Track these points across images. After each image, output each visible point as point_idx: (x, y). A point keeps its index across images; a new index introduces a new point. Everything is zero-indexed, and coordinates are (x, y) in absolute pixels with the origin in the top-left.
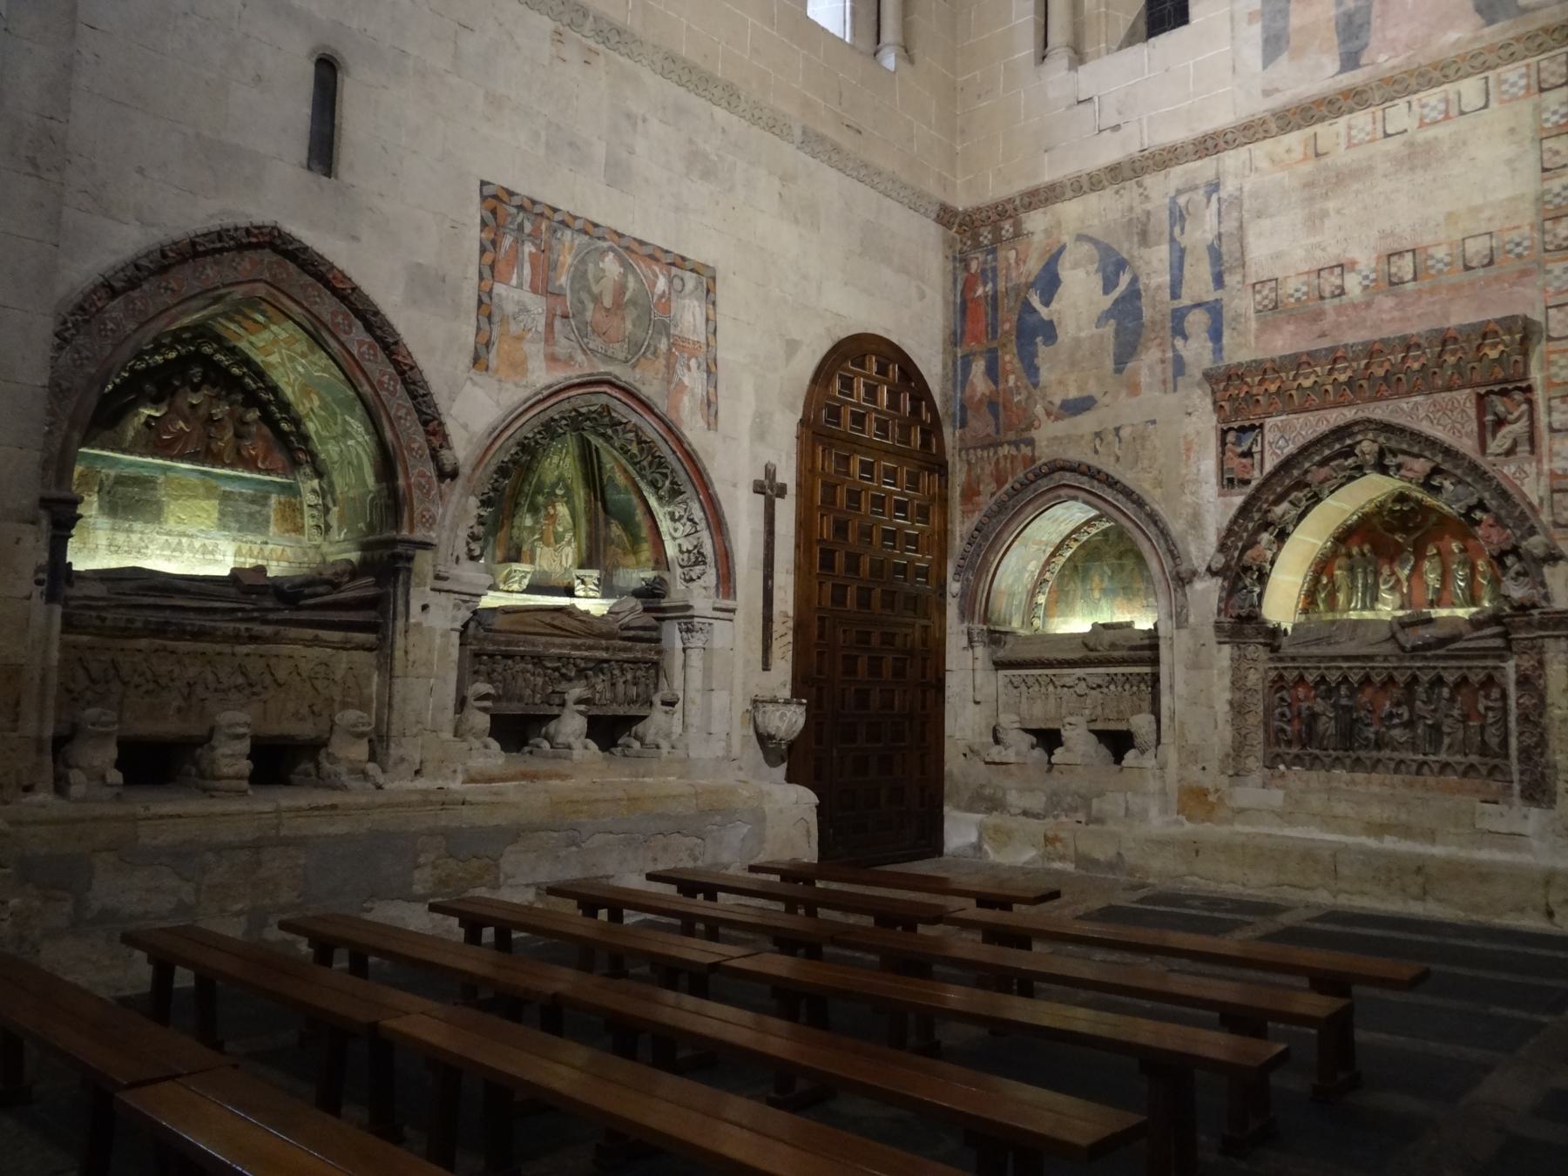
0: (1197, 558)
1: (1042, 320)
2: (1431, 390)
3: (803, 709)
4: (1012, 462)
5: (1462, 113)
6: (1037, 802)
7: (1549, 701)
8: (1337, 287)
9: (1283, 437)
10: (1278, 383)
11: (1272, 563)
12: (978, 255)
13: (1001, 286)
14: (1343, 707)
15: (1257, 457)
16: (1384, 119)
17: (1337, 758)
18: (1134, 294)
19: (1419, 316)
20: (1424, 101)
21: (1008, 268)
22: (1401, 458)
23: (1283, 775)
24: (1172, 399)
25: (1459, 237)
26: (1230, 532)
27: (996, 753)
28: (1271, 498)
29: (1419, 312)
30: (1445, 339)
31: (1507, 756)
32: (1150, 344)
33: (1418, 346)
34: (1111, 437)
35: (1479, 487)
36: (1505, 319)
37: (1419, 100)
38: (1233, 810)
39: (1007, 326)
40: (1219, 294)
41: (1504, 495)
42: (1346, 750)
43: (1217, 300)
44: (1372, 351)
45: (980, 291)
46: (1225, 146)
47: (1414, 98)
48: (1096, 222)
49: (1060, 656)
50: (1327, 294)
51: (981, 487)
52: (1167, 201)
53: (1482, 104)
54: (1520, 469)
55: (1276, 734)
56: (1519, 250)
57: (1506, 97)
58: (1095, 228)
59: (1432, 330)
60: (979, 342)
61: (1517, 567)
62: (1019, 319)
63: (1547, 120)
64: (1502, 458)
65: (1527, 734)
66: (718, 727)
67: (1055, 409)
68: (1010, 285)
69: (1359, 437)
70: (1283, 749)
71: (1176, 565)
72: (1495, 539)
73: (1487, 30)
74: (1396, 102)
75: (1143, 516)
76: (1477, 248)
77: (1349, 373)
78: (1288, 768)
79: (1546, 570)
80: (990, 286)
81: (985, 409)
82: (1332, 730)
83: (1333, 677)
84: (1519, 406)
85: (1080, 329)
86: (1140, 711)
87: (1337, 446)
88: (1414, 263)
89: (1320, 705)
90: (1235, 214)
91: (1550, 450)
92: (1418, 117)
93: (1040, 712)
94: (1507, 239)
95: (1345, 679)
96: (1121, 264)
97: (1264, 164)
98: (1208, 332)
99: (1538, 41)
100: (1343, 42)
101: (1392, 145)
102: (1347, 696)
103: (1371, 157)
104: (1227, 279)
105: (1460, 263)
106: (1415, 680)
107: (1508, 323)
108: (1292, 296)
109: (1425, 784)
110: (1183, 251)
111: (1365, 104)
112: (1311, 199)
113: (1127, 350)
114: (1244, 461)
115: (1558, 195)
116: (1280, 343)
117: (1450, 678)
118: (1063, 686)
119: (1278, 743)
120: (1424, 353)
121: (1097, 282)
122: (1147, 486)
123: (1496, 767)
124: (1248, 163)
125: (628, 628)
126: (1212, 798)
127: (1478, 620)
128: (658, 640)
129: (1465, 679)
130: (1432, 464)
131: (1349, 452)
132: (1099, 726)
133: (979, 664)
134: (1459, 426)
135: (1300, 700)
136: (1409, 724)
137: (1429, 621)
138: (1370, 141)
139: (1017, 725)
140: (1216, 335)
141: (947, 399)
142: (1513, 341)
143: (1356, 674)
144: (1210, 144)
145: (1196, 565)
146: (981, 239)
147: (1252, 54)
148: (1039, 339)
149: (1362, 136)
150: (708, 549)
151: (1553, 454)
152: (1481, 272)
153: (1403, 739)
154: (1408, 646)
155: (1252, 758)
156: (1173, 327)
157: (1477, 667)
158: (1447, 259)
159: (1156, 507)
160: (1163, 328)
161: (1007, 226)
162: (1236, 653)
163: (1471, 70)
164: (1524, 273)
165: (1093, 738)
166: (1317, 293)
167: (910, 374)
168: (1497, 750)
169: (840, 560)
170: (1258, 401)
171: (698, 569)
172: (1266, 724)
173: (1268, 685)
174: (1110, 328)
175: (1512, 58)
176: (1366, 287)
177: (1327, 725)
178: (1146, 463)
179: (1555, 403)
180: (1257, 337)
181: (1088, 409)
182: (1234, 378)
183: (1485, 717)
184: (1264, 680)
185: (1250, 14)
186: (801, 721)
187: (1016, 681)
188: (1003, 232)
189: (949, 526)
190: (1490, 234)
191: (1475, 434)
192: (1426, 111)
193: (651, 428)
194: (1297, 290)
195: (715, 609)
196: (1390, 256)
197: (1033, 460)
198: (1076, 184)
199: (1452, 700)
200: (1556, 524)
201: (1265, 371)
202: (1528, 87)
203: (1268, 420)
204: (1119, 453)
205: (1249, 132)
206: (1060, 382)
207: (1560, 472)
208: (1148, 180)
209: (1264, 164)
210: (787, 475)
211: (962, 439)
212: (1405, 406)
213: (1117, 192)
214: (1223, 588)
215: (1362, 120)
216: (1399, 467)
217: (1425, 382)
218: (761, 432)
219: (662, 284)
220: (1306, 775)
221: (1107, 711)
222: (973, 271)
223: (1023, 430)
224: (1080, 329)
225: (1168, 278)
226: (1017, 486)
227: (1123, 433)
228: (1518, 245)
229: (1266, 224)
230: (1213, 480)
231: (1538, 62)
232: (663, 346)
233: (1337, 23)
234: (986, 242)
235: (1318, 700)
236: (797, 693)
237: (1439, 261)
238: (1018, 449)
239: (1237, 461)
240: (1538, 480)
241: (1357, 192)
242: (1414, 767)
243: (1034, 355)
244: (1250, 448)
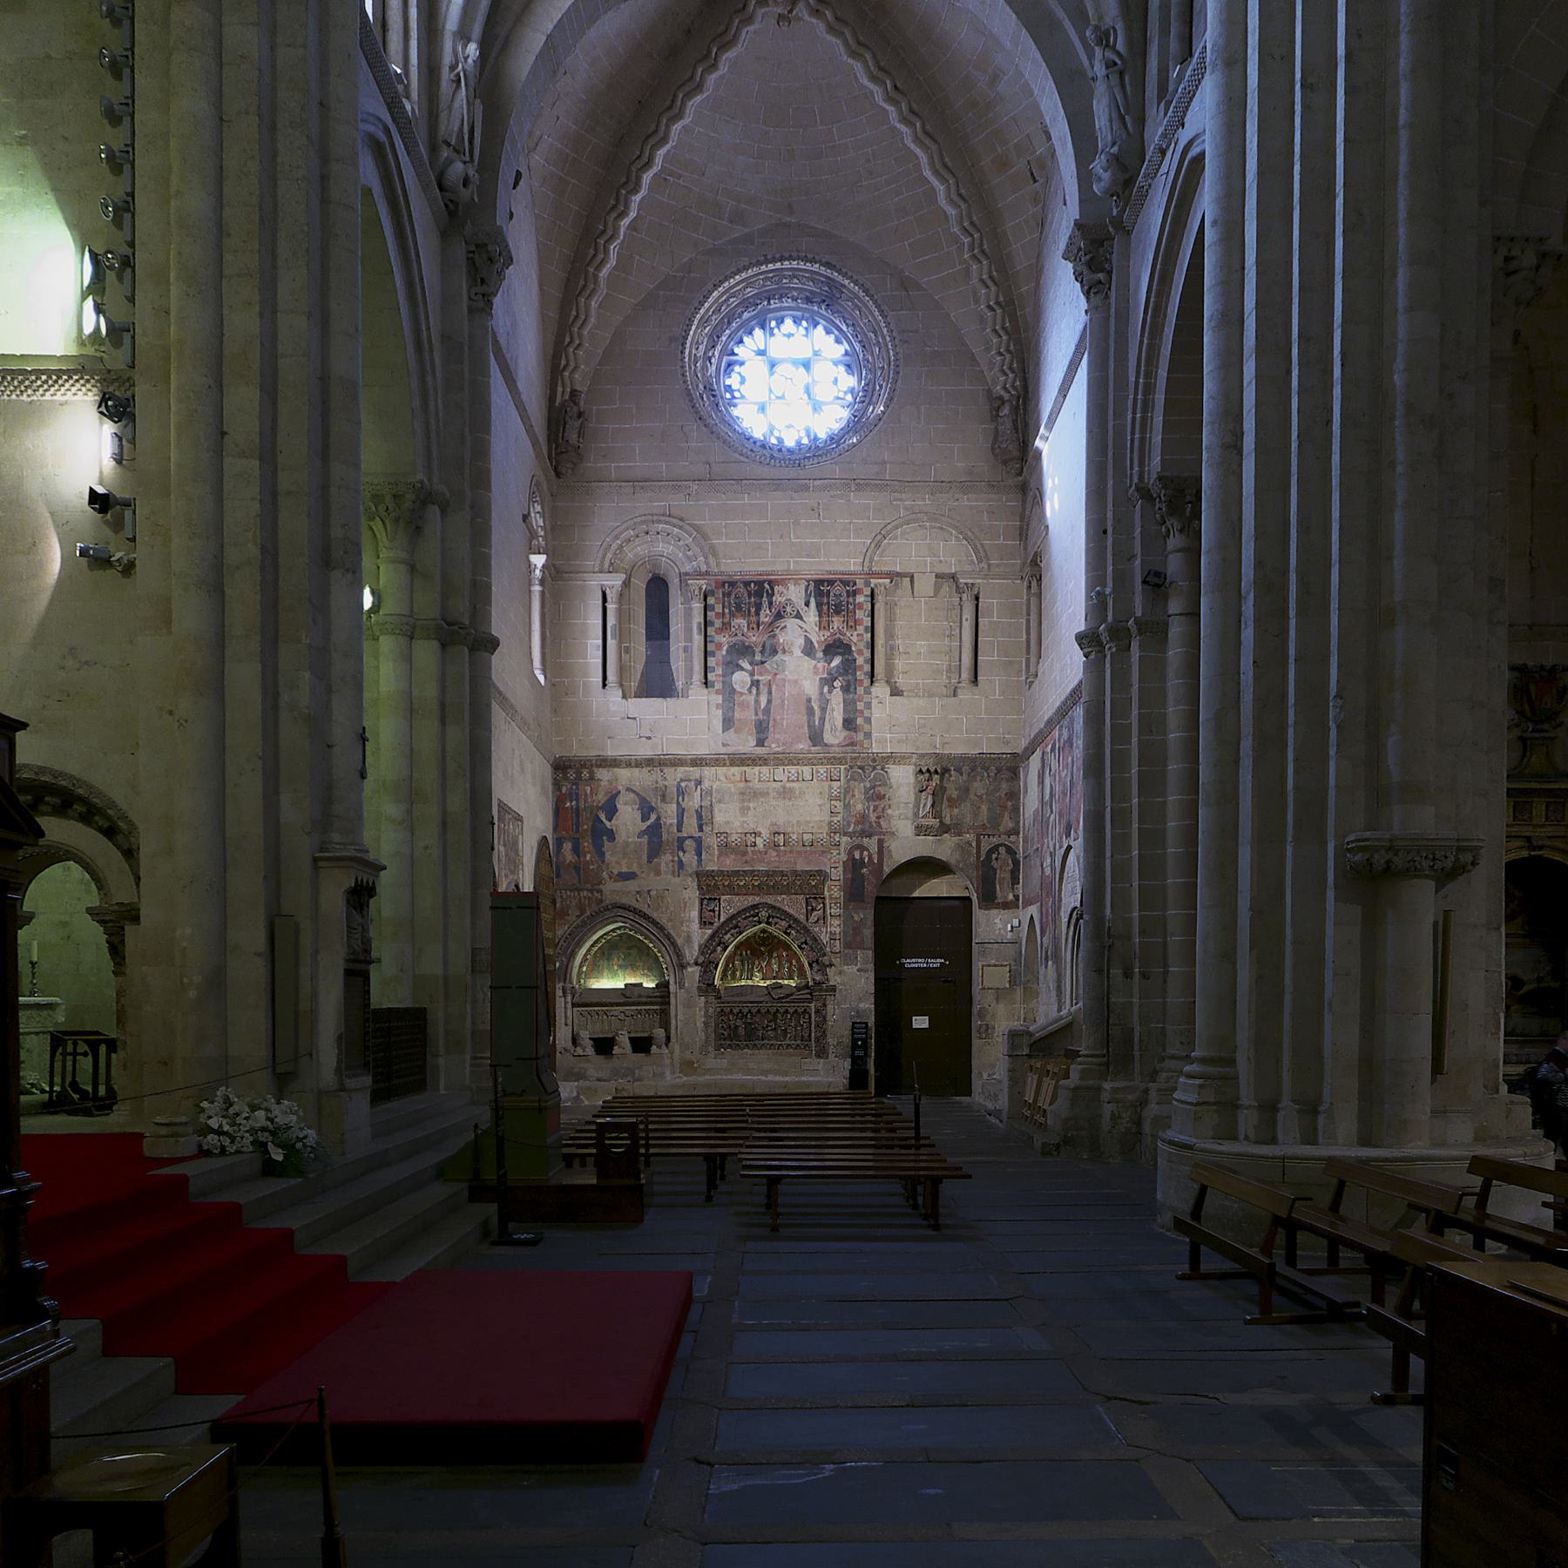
2: (788, 893)
6: (601, 1075)
13: (582, 805)
18: (657, 825)
21: (586, 795)
22: (776, 919)
23: (723, 1053)
24: (677, 880)
26: (706, 946)
27: (579, 1051)
30: (796, 873)
39: (586, 827)
40: (700, 834)
41: (815, 939)
44: (767, 873)
45: (568, 804)
58: (637, 786)
71: (679, 959)
80: (574, 803)
86: (654, 1027)
93: (602, 1030)
95: (750, 1011)
96: (652, 809)
97: (723, 778)
100: (757, 733)
107: (820, 872)
110: (683, 809)
111: (766, 764)
112: (743, 800)
113: (655, 850)
117: (791, 1011)
121: (638, 815)
129: (796, 1011)
137: (781, 986)
140: (699, 854)
147: (718, 725)
148: (604, 838)
151: (831, 925)
161: (585, 774)
164: (823, 852)
174: (645, 840)
177: (741, 1031)
187: (585, 1014)
197: (602, 901)
205: (716, 761)
206: (617, 862)
208: (666, 770)
215: (765, 769)
216: (776, 924)
217: (787, 890)
227: (651, 893)
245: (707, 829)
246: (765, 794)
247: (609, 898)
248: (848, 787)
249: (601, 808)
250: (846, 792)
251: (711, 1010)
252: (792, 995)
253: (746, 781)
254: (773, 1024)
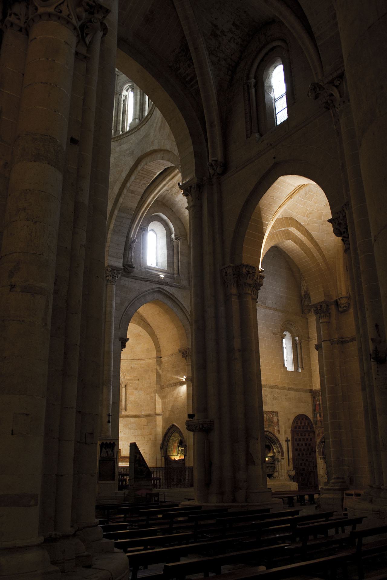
3: (295, 472)
45: (317, 403)
66: (283, 475)
80: (319, 402)
125: (270, 462)
128: (274, 463)
133: (322, 462)
150: (280, 450)
167: (307, 418)
169: (298, 449)
171: (279, 453)
186: (295, 473)
193: (272, 436)
195: (282, 459)
210: (290, 438)
218: (286, 433)
219: (271, 416)
232: (272, 424)
236: (294, 469)
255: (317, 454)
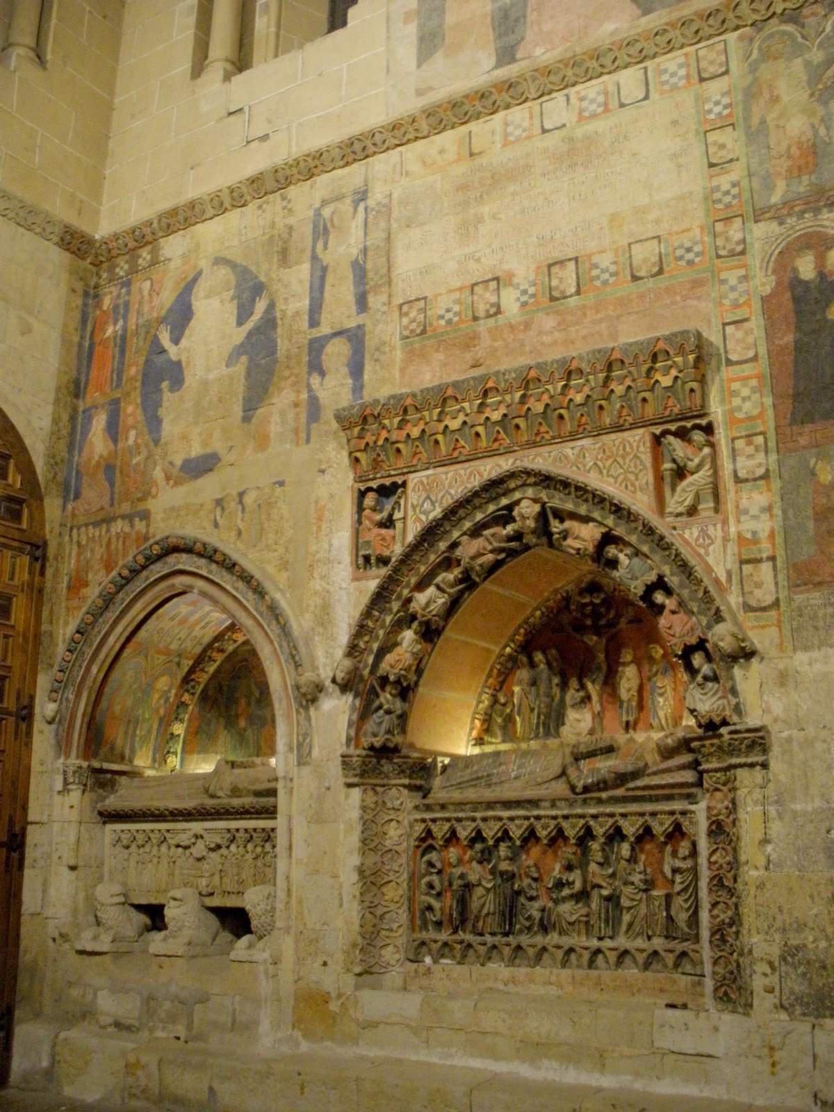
0: (325, 665)
1: (170, 361)
2: (600, 431)
4: (124, 542)
5: (622, 105)
7: (743, 858)
8: (492, 305)
9: (428, 497)
10: (421, 426)
11: (419, 672)
12: (113, 289)
14: (502, 874)
15: (399, 525)
16: (542, 114)
17: (494, 947)
18: (269, 322)
19: (584, 338)
20: (583, 93)
21: (141, 303)
22: (568, 524)
25: (625, 242)
28: (413, 580)
29: (584, 332)
31: (697, 938)
32: (283, 384)
33: (580, 372)
34: (233, 505)
35: (657, 558)
36: (675, 335)
37: (578, 93)
38: (357, 1022)
39: (133, 371)
40: (361, 319)
41: (685, 568)
42: (506, 934)
43: (359, 327)
45: (110, 331)
46: (372, 149)
47: (572, 91)
48: (236, 243)
49: (173, 804)
50: (481, 314)
51: (90, 576)
52: (311, 213)
53: (642, 96)
54: (704, 533)
55: (423, 913)
56: (690, 256)
57: (666, 87)
59: (594, 352)
60: (103, 393)
61: (706, 669)
62: (147, 361)
63: (710, 111)
64: (684, 519)
65: (721, 906)
67: (175, 472)
68: (141, 321)
69: (517, 495)
70: (431, 934)
72: (677, 630)
73: (644, 20)
74: (554, 95)
75: (264, 609)
76: (644, 255)
77: (503, 410)
78: (435, 961)
79: (737, 671)
80: (121, 323)
81: (101, 476)
82: (490, 907)
83: (490, 831)
84: (700, 450)
85: (209, 370)
87: (491, 508)
88: (577, 274)
89: (475, 872)
90: (383, 224)
91: (737, 507)
92: (577, 110)
94: (676, 244)
95: (506, 832)
96: (258, 289)
97: (415, 167)
98: (348, 365)
99: (694, 28)
100: (499, 36)
101: (551, 141)
102: (507, 858)
103: (528, 155)
104: (371, 299)
105: (628, 272)
106: (588, 833)
108: (442, 317)
109: (598, 983)
110: (324, 269)
114: (383, 531)
115: (728, 193)
116: (428, 376)
118: (178, 846)
119: (424, 926)
120: (587, 381)
121: (231, 310)
122: (271, 569)
123: (684, 954)
124: (398, 166)
126: (334, 1006)
127: (666, 746)
129: (648, 830)
130: (604, 530)
131: (505, 517)
132: (216, 902)
134: (632, 477)
135: (450, 864)
136: (582, 896)
138: (528, 138)
139: (122, 899)
140: (356, 370)
141: (53, 461)
142: (686, 362)
143: (519, 827)
144: (357, 147)
145: (323, 676)
146: (117, 270)
147: (407, 52)
148: (165, 385)
149: (517, 133)
152: (650, 283)
153: (574, 918)
154: (580, 785)
155: (390, 948)
156: (310, 361)
157: (662, 813)
158: (613, 268)
159: (278, 596)
160: (299, 363)
162: (371, 799)
163: (629, 60)
164: (697, 283)
165: (213, 921)
166: (470, 313)
168: (686, 930)
170: (398, 451)
172: (411, 900)
173: (413, 843)
175: (670, 47)
176: (524, 304)
177: (484, 901)
178: (271, 537)
179: (740, 444)
180: (402, 370)
181: (211, 470)
182: (370, 420)
183: (673, 882)
184: (409, 836)
185: (406, 13)
188: (140, 261)
189: (45, 627)
190: (658, 237)
191: (651, 487)
192: (585, 104)
194: (448, 311)
196: (550, 266)
197: (146, 538)
198: (216, 202)
199: (633, 860)
200: (748, 608)
201: (405, 411)
202: (688, 77)
203: (412, 476)
204: (241, 525)
206: (184, 437)
207: (749, 536)
208: (292, 191)
209: (415, 167)
211: (74, 515)
212: (569, 452)
213: (260, 207)
214: (353, 708)
215: (518, 115)
216: (565, 535)
220: (460, 970)
221: (225, 880)
222: (105, 308)
223: (139, 500)
224: (209, 370)
225: (307, 302)
226: (126, 573)
228: (689, 250)
229: (415, 234)
230: (346, 557)
231: (697, 50)
233: (493, 18)
234: (122, 273)
235: (474, 864)
237: (603, 271)
238: (132, 526)
239: (376, 531)
240: (725, 547)
241: (514, 194)
242: (586, 956)
243: (158, 404)
244: (391, 515)
245: (374, 301)
246: (517, 173)
247: (163, 527)
248: (756, 80)
249: (162, 321)
250: (751, 94)
251: (393, 832)
252: (635, 775)
253: (471, 155)
254: (576, 877)
255: (42, 740)
